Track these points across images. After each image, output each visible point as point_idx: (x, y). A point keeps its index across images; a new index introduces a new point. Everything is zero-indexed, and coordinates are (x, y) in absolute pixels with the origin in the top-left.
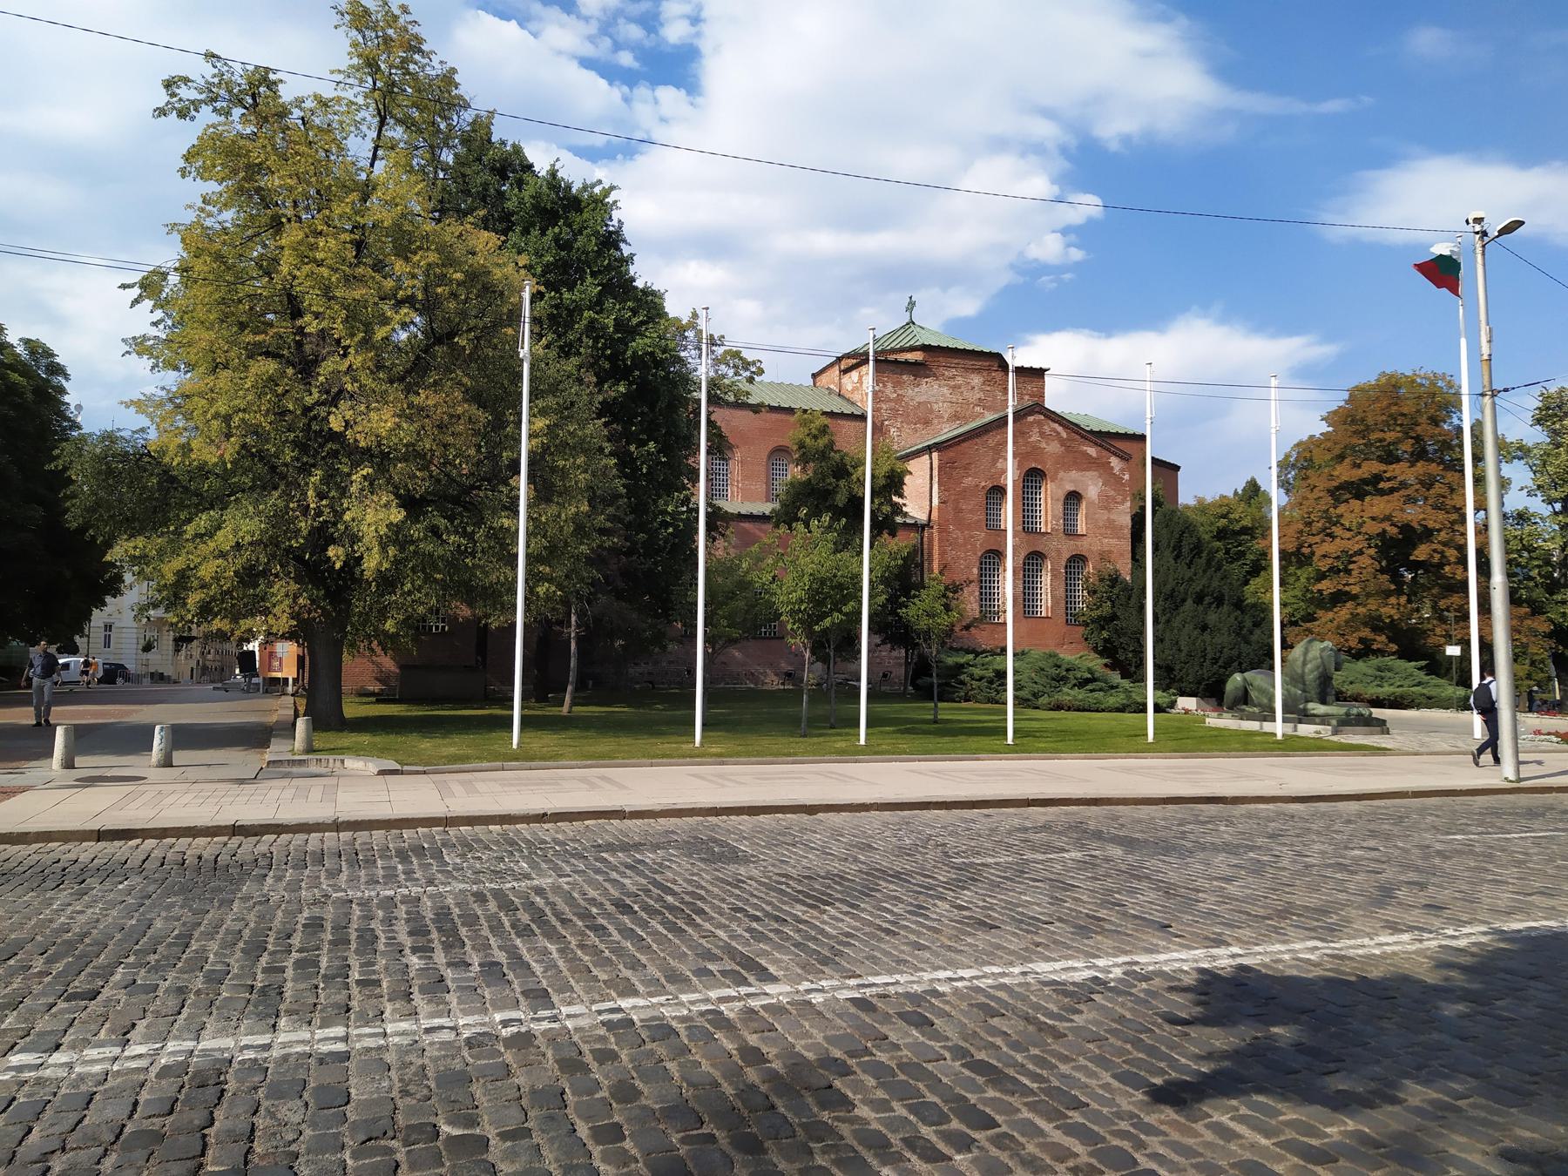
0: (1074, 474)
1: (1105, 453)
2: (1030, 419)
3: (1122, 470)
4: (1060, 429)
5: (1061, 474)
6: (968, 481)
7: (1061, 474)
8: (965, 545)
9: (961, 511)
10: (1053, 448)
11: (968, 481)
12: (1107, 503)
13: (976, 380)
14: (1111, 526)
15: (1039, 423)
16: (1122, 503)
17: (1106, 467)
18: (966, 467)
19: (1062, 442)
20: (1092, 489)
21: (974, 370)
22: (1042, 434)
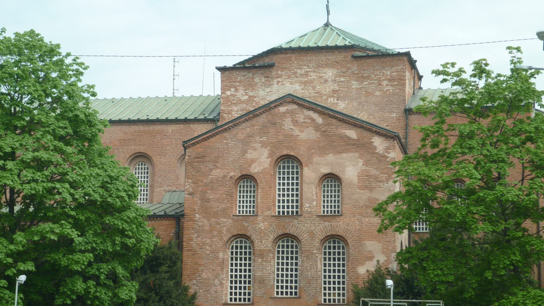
0: (331, 157)
1: (366, 134)
2: (282, 109)
3: (387, 149)
4: (315, 116)
5: (316, 159)
6: (217, 173)
7: (316, 159)
8: (211, 231)
9: (208, 201)
10: (307, 135)
11: (217, 173)
12: (367, 182)
13: (330, 73)
15: (292, 113)
17: (369, 148)
18: (215, 161)
19: (317, 128)
20: (351, 169)
21: (327, 66)
22: (295, 122)
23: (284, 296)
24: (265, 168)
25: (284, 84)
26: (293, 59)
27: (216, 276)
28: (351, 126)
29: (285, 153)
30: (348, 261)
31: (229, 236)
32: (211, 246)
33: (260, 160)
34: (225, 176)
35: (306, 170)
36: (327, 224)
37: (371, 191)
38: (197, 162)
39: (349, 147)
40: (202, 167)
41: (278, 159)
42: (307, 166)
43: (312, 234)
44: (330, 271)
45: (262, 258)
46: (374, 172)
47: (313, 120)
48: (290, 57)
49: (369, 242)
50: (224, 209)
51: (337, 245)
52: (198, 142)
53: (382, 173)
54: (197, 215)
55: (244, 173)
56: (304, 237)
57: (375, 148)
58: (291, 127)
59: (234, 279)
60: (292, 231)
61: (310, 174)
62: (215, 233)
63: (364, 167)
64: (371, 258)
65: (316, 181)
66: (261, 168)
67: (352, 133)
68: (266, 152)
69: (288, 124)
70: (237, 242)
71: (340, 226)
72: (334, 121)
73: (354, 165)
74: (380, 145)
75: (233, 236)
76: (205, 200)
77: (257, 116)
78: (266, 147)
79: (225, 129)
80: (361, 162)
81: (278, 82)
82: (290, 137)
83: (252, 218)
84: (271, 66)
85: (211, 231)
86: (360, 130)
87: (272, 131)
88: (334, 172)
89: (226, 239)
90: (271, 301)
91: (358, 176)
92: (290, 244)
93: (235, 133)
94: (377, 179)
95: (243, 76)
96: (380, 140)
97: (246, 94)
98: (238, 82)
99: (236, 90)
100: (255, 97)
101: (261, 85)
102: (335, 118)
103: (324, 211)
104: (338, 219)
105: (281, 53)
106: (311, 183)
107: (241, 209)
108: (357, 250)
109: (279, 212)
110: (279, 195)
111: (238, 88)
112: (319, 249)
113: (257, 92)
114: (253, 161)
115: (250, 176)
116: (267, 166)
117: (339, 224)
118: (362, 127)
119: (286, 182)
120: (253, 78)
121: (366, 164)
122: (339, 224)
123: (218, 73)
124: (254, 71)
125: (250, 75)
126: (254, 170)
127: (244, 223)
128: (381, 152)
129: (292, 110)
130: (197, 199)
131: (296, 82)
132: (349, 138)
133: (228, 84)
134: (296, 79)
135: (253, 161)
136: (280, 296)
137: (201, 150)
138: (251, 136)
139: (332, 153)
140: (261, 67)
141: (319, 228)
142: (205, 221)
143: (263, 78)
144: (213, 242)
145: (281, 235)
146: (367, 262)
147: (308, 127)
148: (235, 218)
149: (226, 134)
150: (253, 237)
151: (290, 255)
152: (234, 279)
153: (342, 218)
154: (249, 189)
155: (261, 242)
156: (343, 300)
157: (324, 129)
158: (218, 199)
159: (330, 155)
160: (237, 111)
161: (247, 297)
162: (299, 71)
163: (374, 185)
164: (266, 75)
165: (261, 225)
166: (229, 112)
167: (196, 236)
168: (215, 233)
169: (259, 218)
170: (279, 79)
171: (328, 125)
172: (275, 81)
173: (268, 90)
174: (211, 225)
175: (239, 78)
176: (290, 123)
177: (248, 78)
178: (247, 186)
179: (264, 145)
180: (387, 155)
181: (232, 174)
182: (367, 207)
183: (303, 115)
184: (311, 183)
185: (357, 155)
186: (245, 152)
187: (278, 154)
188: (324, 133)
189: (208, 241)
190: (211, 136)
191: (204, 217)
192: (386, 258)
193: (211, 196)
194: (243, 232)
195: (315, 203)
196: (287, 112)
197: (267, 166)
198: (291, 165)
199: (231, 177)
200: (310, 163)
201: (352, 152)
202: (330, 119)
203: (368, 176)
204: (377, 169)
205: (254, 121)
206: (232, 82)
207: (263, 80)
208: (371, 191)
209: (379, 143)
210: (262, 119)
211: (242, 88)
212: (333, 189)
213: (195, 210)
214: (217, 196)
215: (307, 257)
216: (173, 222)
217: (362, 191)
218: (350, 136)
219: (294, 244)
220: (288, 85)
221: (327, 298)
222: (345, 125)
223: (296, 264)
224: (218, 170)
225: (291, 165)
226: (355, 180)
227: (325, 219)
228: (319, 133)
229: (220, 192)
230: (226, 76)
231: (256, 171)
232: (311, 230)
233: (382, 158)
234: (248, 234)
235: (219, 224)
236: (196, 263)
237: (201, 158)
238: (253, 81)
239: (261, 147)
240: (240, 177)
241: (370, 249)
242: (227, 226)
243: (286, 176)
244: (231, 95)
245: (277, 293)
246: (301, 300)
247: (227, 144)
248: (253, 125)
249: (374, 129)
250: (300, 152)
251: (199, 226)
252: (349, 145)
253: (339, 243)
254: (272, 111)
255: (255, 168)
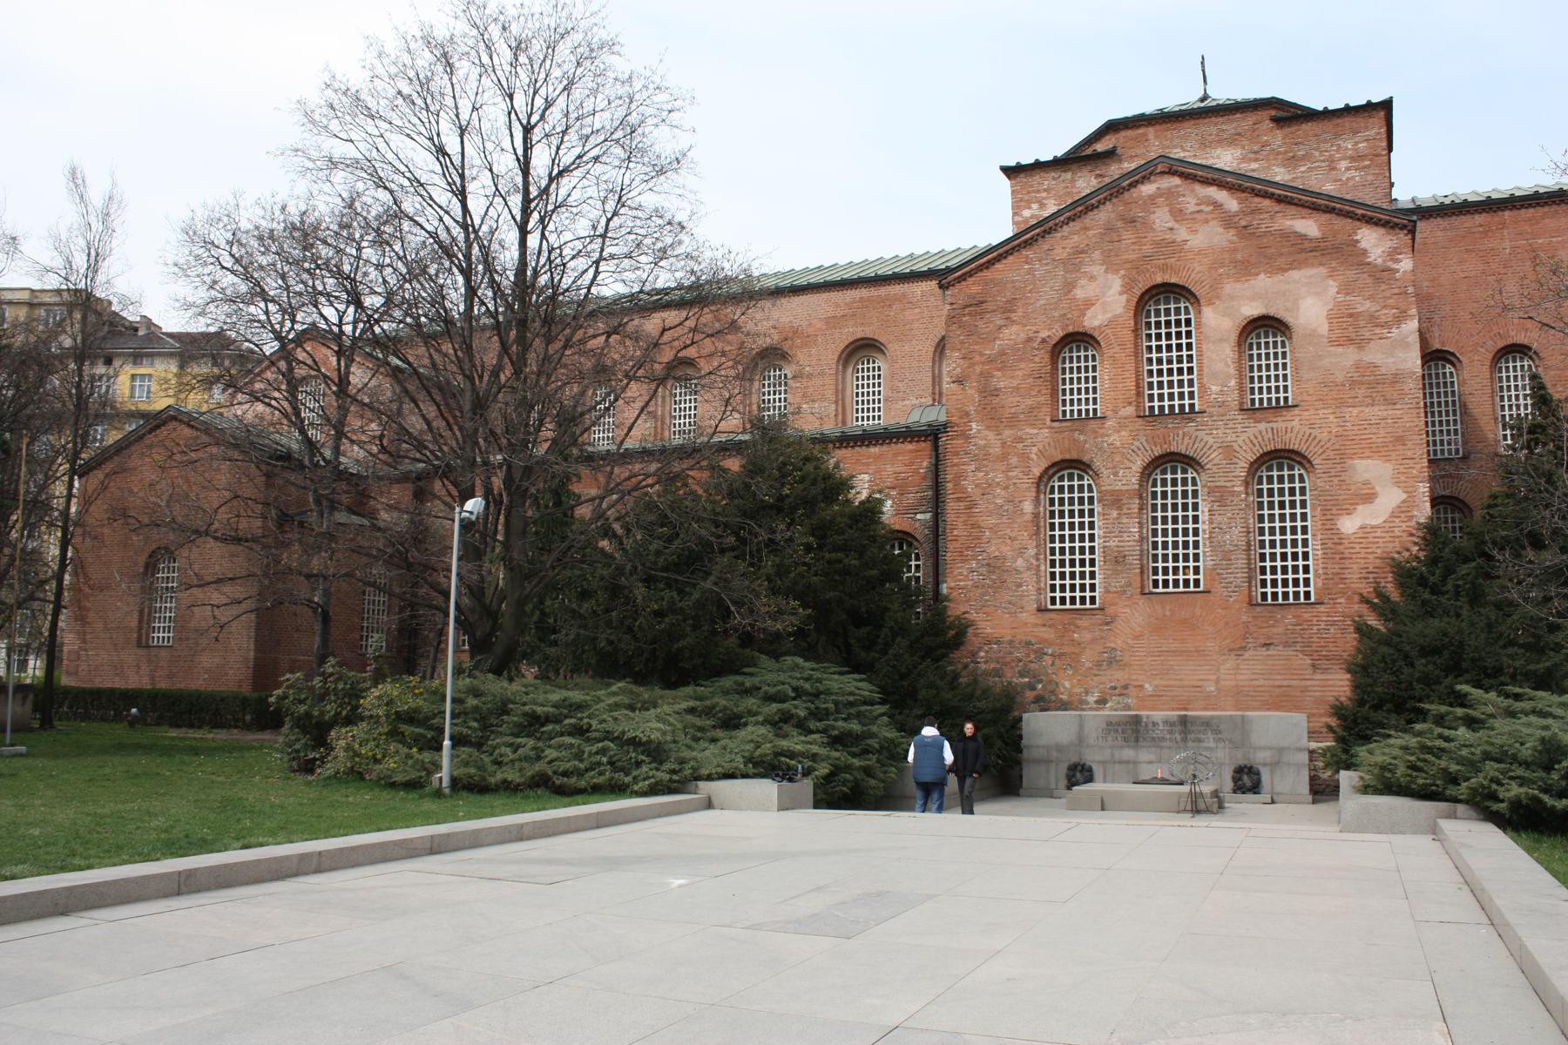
0: (1262, 281)
2: (1147, 189)
3: (1393, 254)
4: (1221, 195)
5: (1229, 288)
6: (1012, 334)
7: (1229, 288)
8: (1004, 457)
9: (996, 393)
10: (1206, 238)
11: (1012, 334)
12: (1350, 328)
14: (1373, 383)
15: (1170, 194)
16: (1400, 319)
17: (1350, 254)
18: (1008, 309)
19: (1228, 221)
20: (1310, 301)
22: (1178, 214)
23: (1171, 589)
24: (1116, 316)
27: (1021, 551)
28: (1305, 211)
29: (1159, 279)
30: (1313, 508)
31: (1044, 465)
32: (1006, 488)
33: (1106, 300)
34: (1030, 340)
35: (1208, 314)
36: (1262, 426)
37: (1361, 348)
38: (970, 314)
39: (1304, 255)
40: (980, 324)
41: (1143, 294)
42: (1210, 303)
43: (1229, 451)
44: (1272, 531)
45: (1120, 508)
46: (1365, 306)
47: (1217, 205)
49: (1364, 462)
50: (1031, 409)
51: (1286, 473)
52: (970, 274)
53: (1385, 307)
54: (974, 425)
55: (1071, 329)
56: (1213, 458)
57: (1365, 252)
58: (1170, 225)
59: (1057, 557)
60: (1181, 447)
61: (1217, 323)
62: (1014, 461)
63: (1341, 298)
64: (1369, 498)
65: (1234, 336)
66: (1109, 315)
67: (1309, 226)
68: (1116, 283)
69: (1161, 218)
70: (1061, 479)
71: (1291, 430)
72: (1267, 202)
73: (1318, 294)
74: (1376, 246)
75: (1054, 465)
76: (989, 392)
77: (1093, 208)
78: (1117, 271)
79: (1025, 242)
80: (1332, 287)
82: (1169, 247)
83: (1093, 424)
85: (1004, 457)
86: (1325, 217)
87: (1128, 236)
88: (1272, 312)
89: (1037, 472)
90: (1142, 601)
91: (1330, 318)
92: (1179, 476)
93: (1046, 247)
94: (1373, 321)
96: (1375, 235)
102: (1266, 195)
103: (1253, 400)
104: (1288, 414)
106: (1221, 340)
107: (1068, 408)
108: (1336, 480)
109: (1151, 408)
110: (1150, 373)
112: (1247, 484)
114: (1089, 303)
115: (1085, 334)
116: (1119, 310)
117: (1289, 425)
118: (1329, 210)
119: (1164, 343)
121: (1346, 289)
122: (1289, 425)
123: (1005, 182)
124: (1074, 167)
126: (1093, 320)
127: (1076, 434)
128: (1379, 261)
129: (1169, 189)
130: (972, 392)
132: (1303, 237)
135: (1089, 303)
136: (1160, 590)
137: (975, 289)
138: (1082, 252)
139: (1266, 272)
141: (1244, 436)
142: (991, 435)
144: (1008, 478)
145: (1161, 457)
146: (1360, 508)
147: (1207, 221)
148: (1056, 424)
149: (1028, 253)
150: (1097, 464)
151: (1180, 501)
152: (1057, 557)
153: (1296, 411)
154: (1083, 364)
155: (1116, 474)
156: (1307, 595)
157: (1243, 223)
158: (1017, 388)
159: (1262, 276)
161: (1088, 594)
163: (1367, 335)
165: (1115, 439)
167: (973, 468)
168: (1014, 461)
169: (1109, 423)
171: (1253, 212)
174: (1004, 444)
176: (1168, 217)
178: (1079, 358)
179: (1111, 266)
180: (1395, 266)
181: (1044, 334)
182: (1354, 383)
183: (1195, 196)
184: (1221, 340)
185: (1323, 270)
186: (1069, 286)
187: (1143, 285)
188: (1245, 232)
189: (1000, 478)
190: (998, 259)
191: (988, 428)
192: (1404, 496)
193: (1001, 382)
194: (1074, 456)
195: (1233, 383)
196: (1160, 193)
197: (1119, 310)
198: (1172, 306)
199: (1044, 341)
200: (1218, 298)
201: (1313, 265)
202: (1257, 200)
203: (1351, 315)
204: (1371, 298)
205: (1088, 220)
208: (1361, 348)
209: (1373, 242)
210: (1104, 215)
212: (1271, 351)
213: (967, 414)
214: (1015, 383)
215: (1221, 501)
216: (926, 446)
217: (1340, 349)
218: (1303, 231)
219: (1189, 476)
221: (1269, 590)
222: (1292, 210)
223: (1196, 519)
224: (1015, 328)
225: (1172, 306)
226: (1324, 329)
227: (1258, 414)
228: (1233, 232)
229: (1020, 373)
231: (1096, 323)
232: (1227, 442)
233: (1382, 274)
234: (1086, 459)
235: (1021, 440)
236: (975, 526)
237: (977, 306)
239: (1106, 271)
240: (1063, 339)
241: (1367, 476)
242: (1041, 443)
243: (1163, 331)
245: (1156, 583)
246: (1211, 597)
247: (1030, 272)
248: (1086, 229)
249: (1360, 212)
250: (1191, 274)
251: (980, 448)
252: (1302, 251)
253: (1291, 468)
254: (1126, 195)
255: (1095, 317)
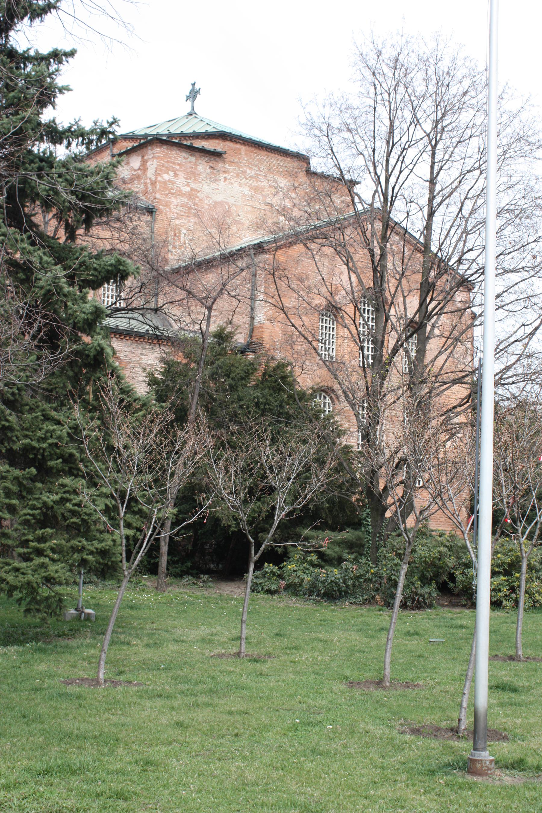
25: (232, 184)
26: (243, 152)
48: (239, 150)
81: (225, 179)
84: (217, 155)
95: (185, 158)
97: (188, 185)
98: (179, 164)
99: (176, 175)
100: (199, 192)
101: (206, 177)
105: (231, 140)
111: (178, 173)
113: (201, 185)
120: (196, 165)
125: (193, 159)
131: (245, 184)
133: (166, 165)
134: (244, 181)
140: (204, 152)
143: (208, 167)
160: (177, 206)
162: (248, 171)
164: (211, 165)
166: (167, 205)
170: (226, 175)
172: (222, 176)
173: (214, 186)
175: (179, 159)
177: (190, 162)
206: (171, 162)
207: (209, 171)
211: (183, 175)
220: (236, 185)
230: (164, 152)
238: (196, 169)
244: (170, 181)
